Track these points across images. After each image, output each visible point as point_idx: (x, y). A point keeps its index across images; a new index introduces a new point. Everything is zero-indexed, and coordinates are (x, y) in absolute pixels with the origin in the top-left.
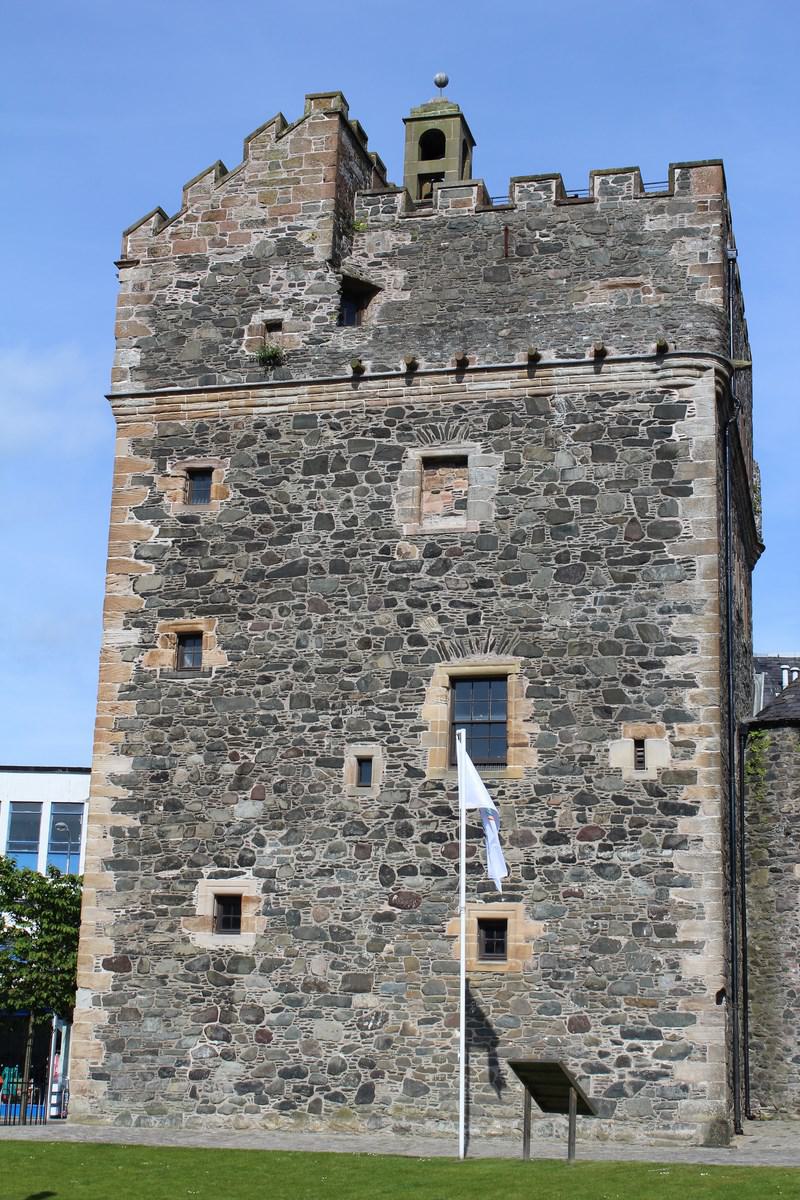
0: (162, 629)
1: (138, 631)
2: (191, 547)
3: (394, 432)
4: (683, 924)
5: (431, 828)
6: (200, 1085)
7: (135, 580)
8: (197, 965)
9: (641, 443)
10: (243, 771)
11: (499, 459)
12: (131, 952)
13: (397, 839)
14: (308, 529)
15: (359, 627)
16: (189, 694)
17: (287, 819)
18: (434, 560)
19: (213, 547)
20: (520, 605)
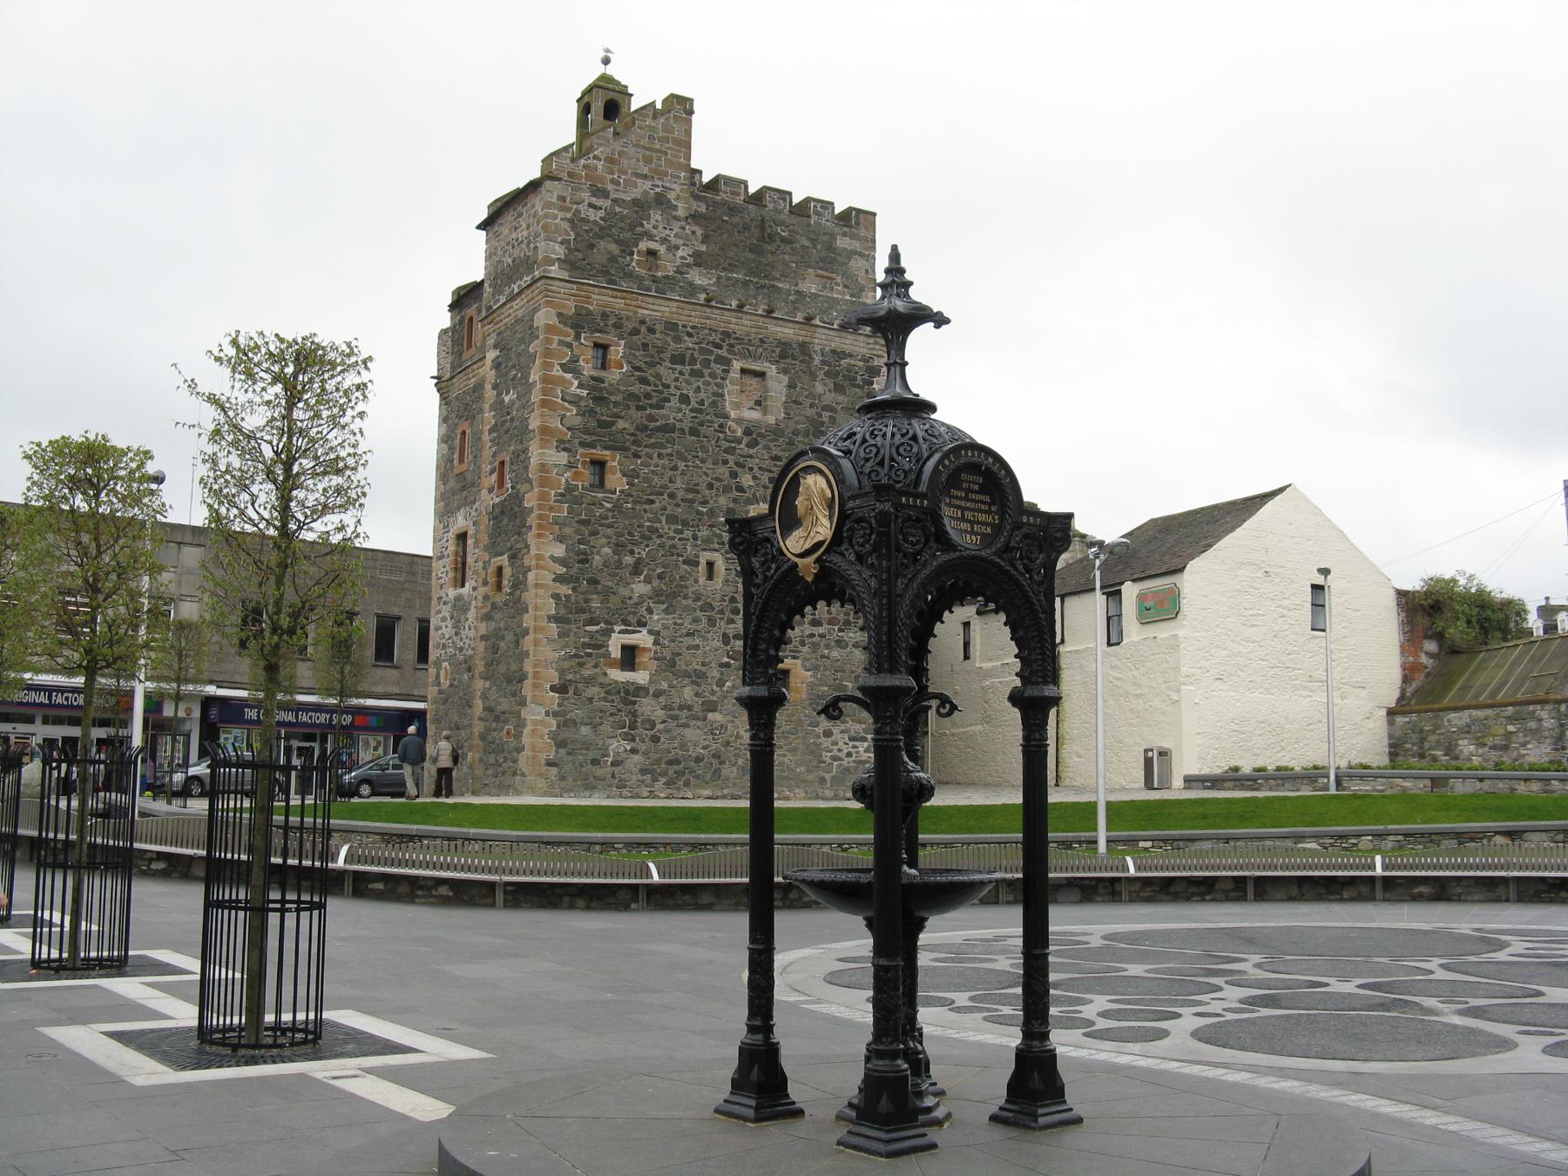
2: (600, 400)
6: (616, 770)
9: (858, 386)
10: (638, 562)
11: (785, 379)
14: (674, 402)
17: (668, 596)
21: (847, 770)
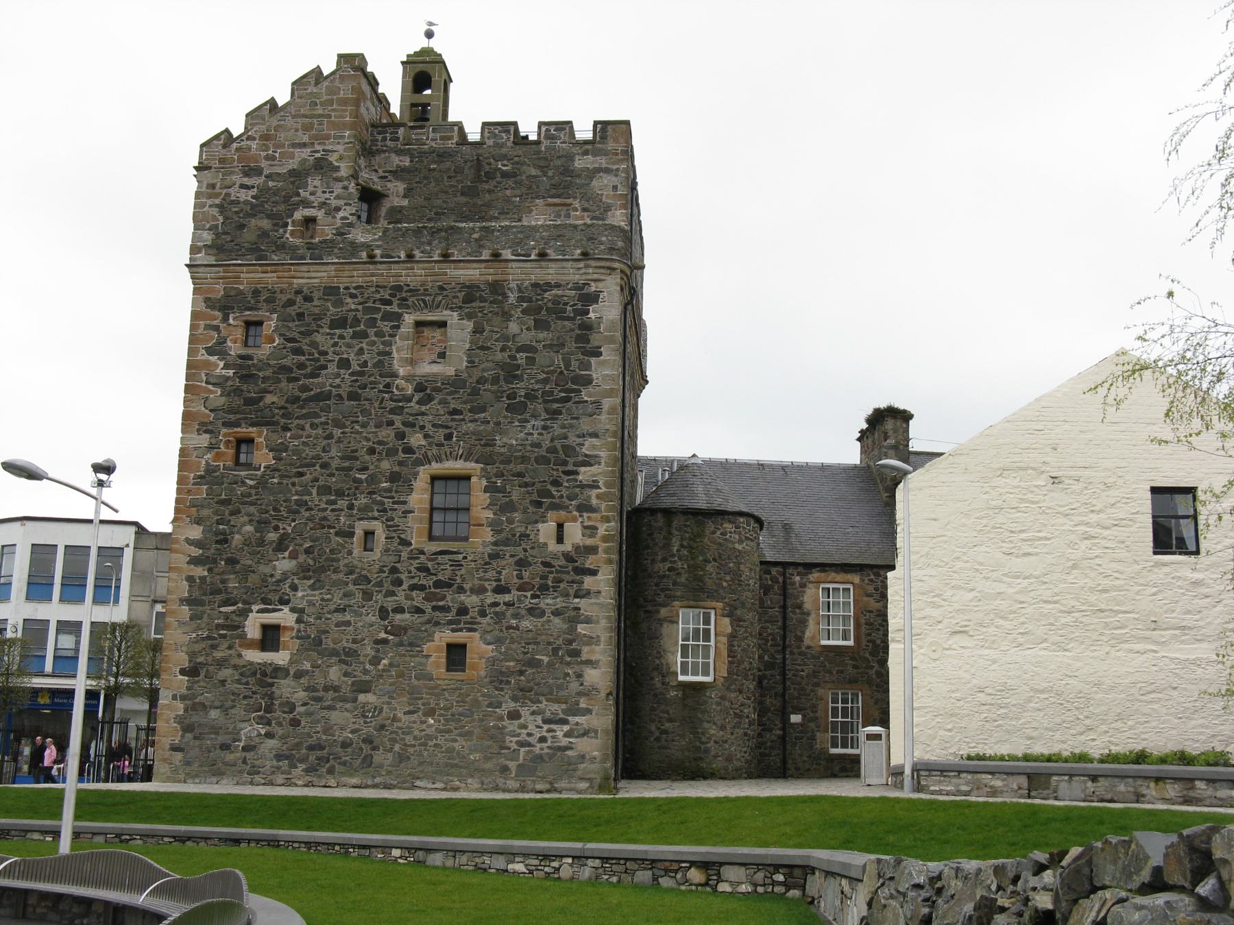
0: (225, 436)
1: (207, 436)
2: (247, 377)
3: (396, 302)
4: (585, 649)
5: (415, 581)
6: (249, 755)
8: (248, 673)
9: (568, 319)
10: (283, 538)
11: (469, 325)
13: (391, 588)
14: (332, 368)
15: (368, 440)
16: (243, 482)
17: (316, 571)
18: (421, 394)
20: (482, 428)
21: (540, 758)
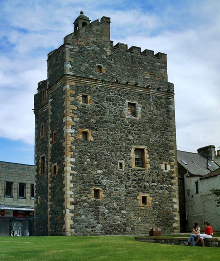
2: (84, 113)
4: (174, 199)
6: (93, 229)
7: (73, 119)
9: (164, 108)
10: (98, 164)
12: (78, 201)
14: (108, 114)
16: (86, 145)
17: (107, 174)
19: (89, 114)
